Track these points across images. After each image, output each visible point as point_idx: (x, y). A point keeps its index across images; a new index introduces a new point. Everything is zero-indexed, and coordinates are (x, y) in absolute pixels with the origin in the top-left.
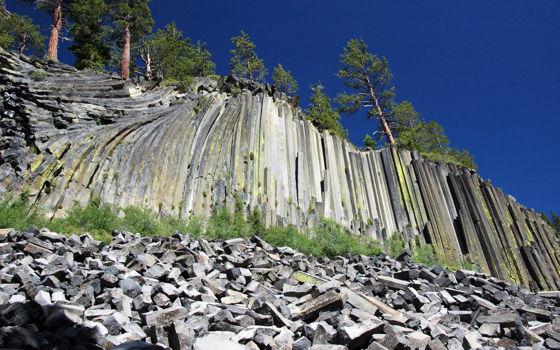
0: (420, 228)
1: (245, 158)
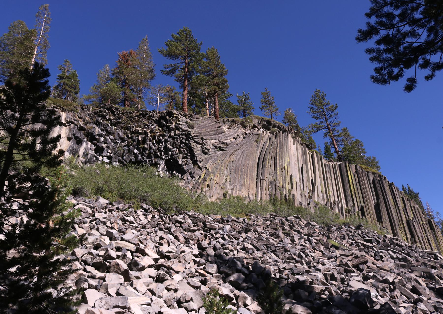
1: (282, 169)
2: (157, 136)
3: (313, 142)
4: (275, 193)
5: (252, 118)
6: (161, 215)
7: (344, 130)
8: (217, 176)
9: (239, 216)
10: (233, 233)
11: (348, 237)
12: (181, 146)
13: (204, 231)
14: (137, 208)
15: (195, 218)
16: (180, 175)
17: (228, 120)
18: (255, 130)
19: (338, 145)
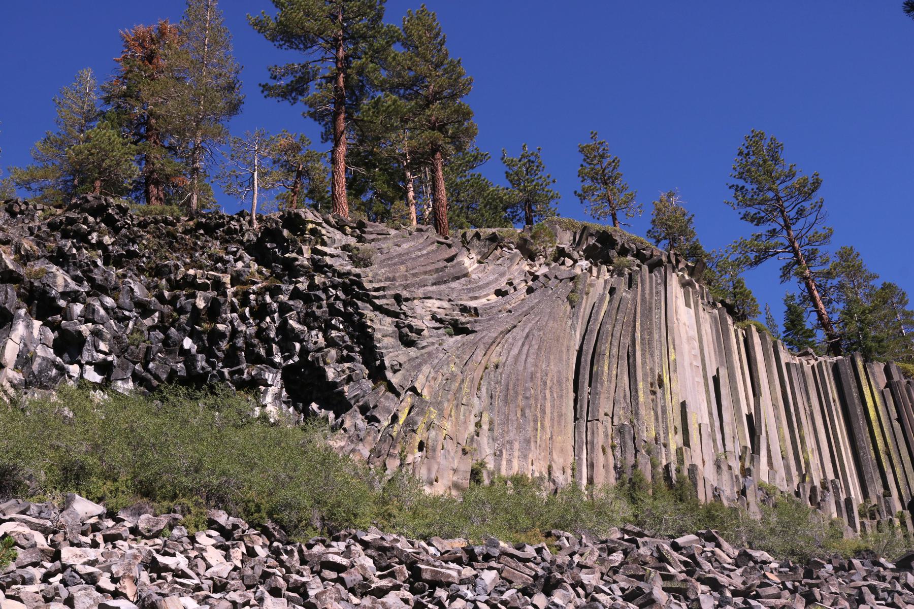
0: (905, 498)
1: (652, 384)
2: (254, 293)
3: (747, 296)
4: (633, 462)
5: (554, 228)
6: (275, 544)
7: (846, 255)
8: (450, 415)
9: (522, 538)
10: (506, 596)
11: (873, 597)
12: (333, 322)
13: (413, 591)
14: (197, 527)
15: (383, 550)
16: (331, 415)
17: (477, 235)
18: (563, 263)
19: (828, 303)
